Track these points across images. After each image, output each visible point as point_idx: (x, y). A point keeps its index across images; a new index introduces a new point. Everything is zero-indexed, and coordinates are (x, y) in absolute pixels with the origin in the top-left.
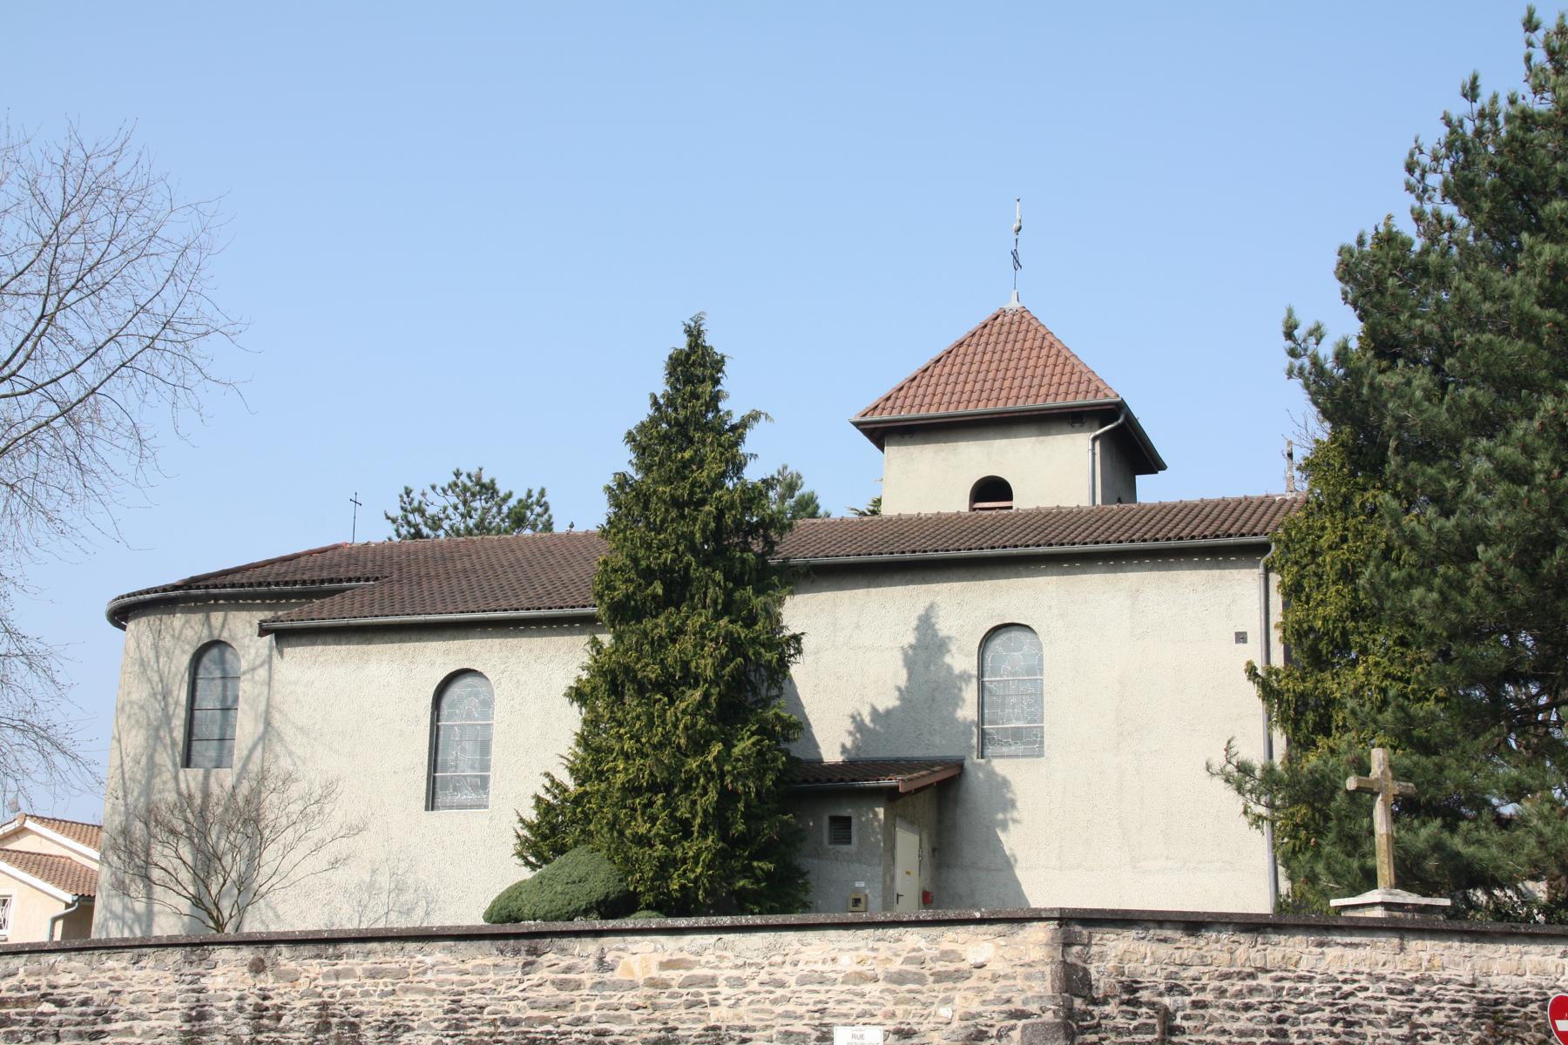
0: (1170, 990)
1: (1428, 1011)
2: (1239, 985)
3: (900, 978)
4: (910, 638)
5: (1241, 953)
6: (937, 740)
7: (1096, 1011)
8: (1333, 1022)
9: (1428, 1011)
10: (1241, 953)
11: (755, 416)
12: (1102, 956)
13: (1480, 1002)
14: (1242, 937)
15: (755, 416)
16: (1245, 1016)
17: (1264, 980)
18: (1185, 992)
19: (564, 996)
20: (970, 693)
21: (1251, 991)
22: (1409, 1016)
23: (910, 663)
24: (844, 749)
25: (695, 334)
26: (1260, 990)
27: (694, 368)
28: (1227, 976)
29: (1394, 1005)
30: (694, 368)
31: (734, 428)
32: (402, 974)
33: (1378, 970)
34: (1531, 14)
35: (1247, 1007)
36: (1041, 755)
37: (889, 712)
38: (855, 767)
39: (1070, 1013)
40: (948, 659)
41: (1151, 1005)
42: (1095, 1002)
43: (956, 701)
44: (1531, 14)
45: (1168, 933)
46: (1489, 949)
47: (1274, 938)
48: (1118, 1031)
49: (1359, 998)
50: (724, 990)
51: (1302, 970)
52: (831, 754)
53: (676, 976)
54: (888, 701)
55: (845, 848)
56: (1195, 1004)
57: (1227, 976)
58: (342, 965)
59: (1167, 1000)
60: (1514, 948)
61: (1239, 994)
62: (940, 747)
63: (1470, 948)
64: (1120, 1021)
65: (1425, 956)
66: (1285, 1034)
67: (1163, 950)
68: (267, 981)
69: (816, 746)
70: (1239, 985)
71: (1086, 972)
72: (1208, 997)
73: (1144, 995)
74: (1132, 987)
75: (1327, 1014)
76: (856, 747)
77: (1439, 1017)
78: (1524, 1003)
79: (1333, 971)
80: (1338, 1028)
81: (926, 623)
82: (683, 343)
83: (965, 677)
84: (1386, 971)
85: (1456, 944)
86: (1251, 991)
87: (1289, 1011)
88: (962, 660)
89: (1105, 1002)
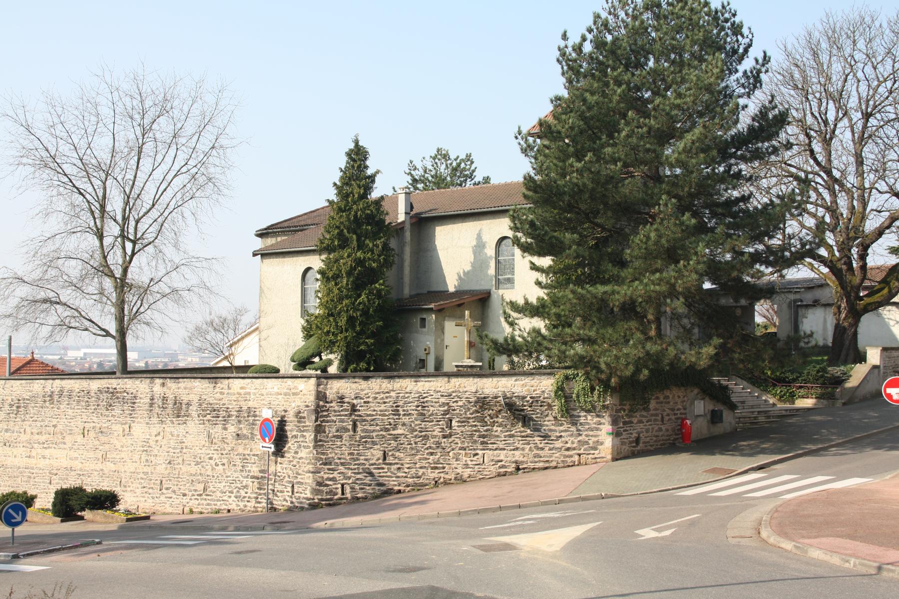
0: (356, 398)
1: (456, 402)
2: (382, 395)
3: (286, 394)
4: (474, 243)
5: (384, 386)
6: (483, 282)
7: (328, 405)
8: (418, 406)
9: (456, 402)
10: (384, 386)
11: (378, 172)
12: (331, 388)
13: (478, 398)
14: (385, 380)
15: (378, 172)
16: (383, 405)
17: (393, 394)
18: (361, 398)
19: (221, 396)
20: (492, 264)
21: (387, 397)
22: (448, 404)
23: (475, 253)
24: (455, 287)
25: (357, 142)
26: (390, 397)
27: (358, 155)
28: (378, 393)
29: (443, 400)
30: (358, 155)
31: (369, 177)
32: (191, 389)
33: (438, 389)
34: (565, 33)
35: (385, 403)
36: (513, 288)
37: (468, 272)
38: (458, 293)
39: (318, 406)
40: (486, 251)
41: (349, 403)
42: (327, 402)
43: (488, 267)
44: (565, 33)
45: (357, 380)
46: (485, 380)
47: (397, 380)
48: (335, 411)
49: (429, 399)
50: (252, 396)
51: (408, 390)
52: (451, 289)
53: (242, 391)
54: (468, 268)
55: (424, 330)
56: (365, 402)
57: (378, 393)
58: (180, 385)
59: (355, 401)
60: (495, 379)
61: (382, 398)
62: (482, 286)
63: (476, 380)
64: (336, 408)
65: (458, 384)
66: (398, 411)
67: (354, 386)
68: (165, 389)
69: (447, 285)
70: (382, 395)
71: (325, 393)
72: (370, 400)
73: (346, 400)
74: (342, 398)
75: (416, 404)
76: (459, 286)
77: (460, 403)
78: (496, 397)
79: (420, 390)
80: (420, 408)
81: (479, 237)
82: (352, 146)
83: (491, 257)
84: (441, 389)
85: (471, 379)
86: (387, 397)
87: (401, 403)
88: (490, 251)
89: (331, 402)
